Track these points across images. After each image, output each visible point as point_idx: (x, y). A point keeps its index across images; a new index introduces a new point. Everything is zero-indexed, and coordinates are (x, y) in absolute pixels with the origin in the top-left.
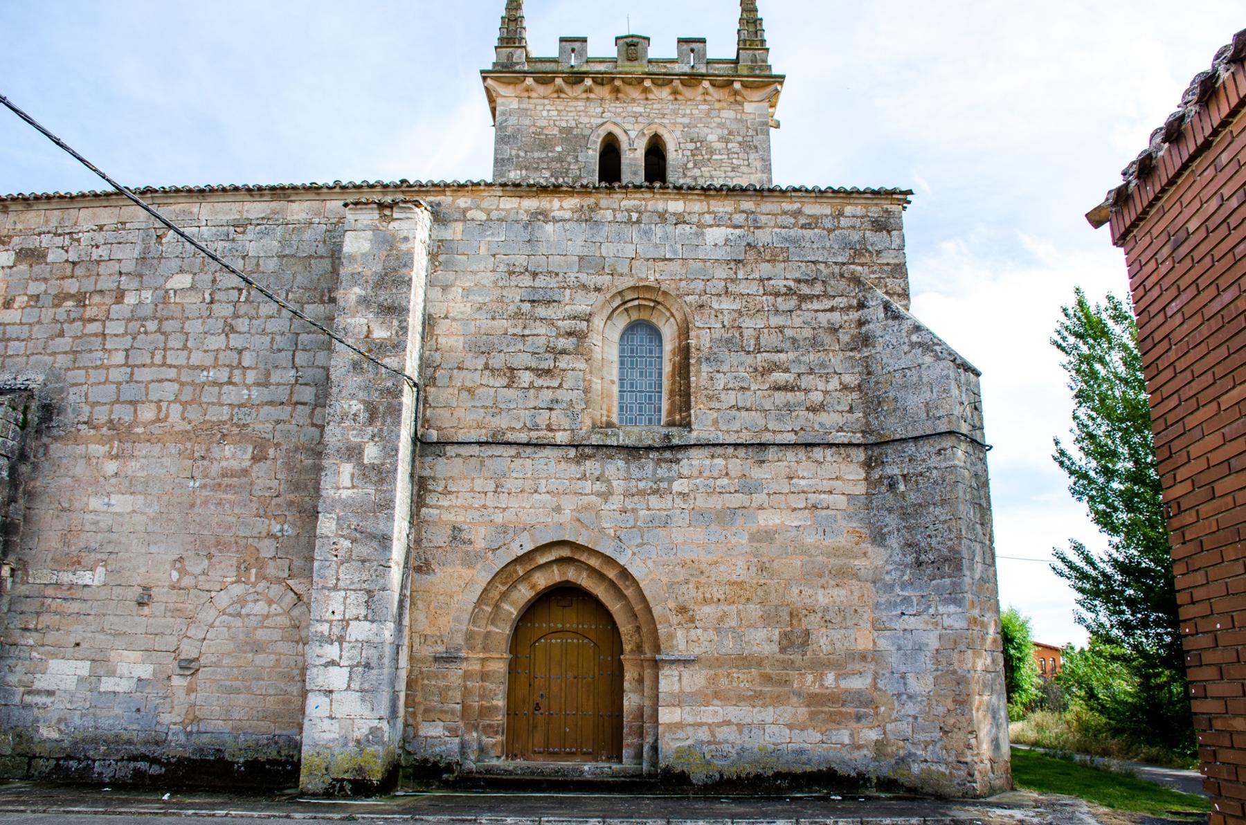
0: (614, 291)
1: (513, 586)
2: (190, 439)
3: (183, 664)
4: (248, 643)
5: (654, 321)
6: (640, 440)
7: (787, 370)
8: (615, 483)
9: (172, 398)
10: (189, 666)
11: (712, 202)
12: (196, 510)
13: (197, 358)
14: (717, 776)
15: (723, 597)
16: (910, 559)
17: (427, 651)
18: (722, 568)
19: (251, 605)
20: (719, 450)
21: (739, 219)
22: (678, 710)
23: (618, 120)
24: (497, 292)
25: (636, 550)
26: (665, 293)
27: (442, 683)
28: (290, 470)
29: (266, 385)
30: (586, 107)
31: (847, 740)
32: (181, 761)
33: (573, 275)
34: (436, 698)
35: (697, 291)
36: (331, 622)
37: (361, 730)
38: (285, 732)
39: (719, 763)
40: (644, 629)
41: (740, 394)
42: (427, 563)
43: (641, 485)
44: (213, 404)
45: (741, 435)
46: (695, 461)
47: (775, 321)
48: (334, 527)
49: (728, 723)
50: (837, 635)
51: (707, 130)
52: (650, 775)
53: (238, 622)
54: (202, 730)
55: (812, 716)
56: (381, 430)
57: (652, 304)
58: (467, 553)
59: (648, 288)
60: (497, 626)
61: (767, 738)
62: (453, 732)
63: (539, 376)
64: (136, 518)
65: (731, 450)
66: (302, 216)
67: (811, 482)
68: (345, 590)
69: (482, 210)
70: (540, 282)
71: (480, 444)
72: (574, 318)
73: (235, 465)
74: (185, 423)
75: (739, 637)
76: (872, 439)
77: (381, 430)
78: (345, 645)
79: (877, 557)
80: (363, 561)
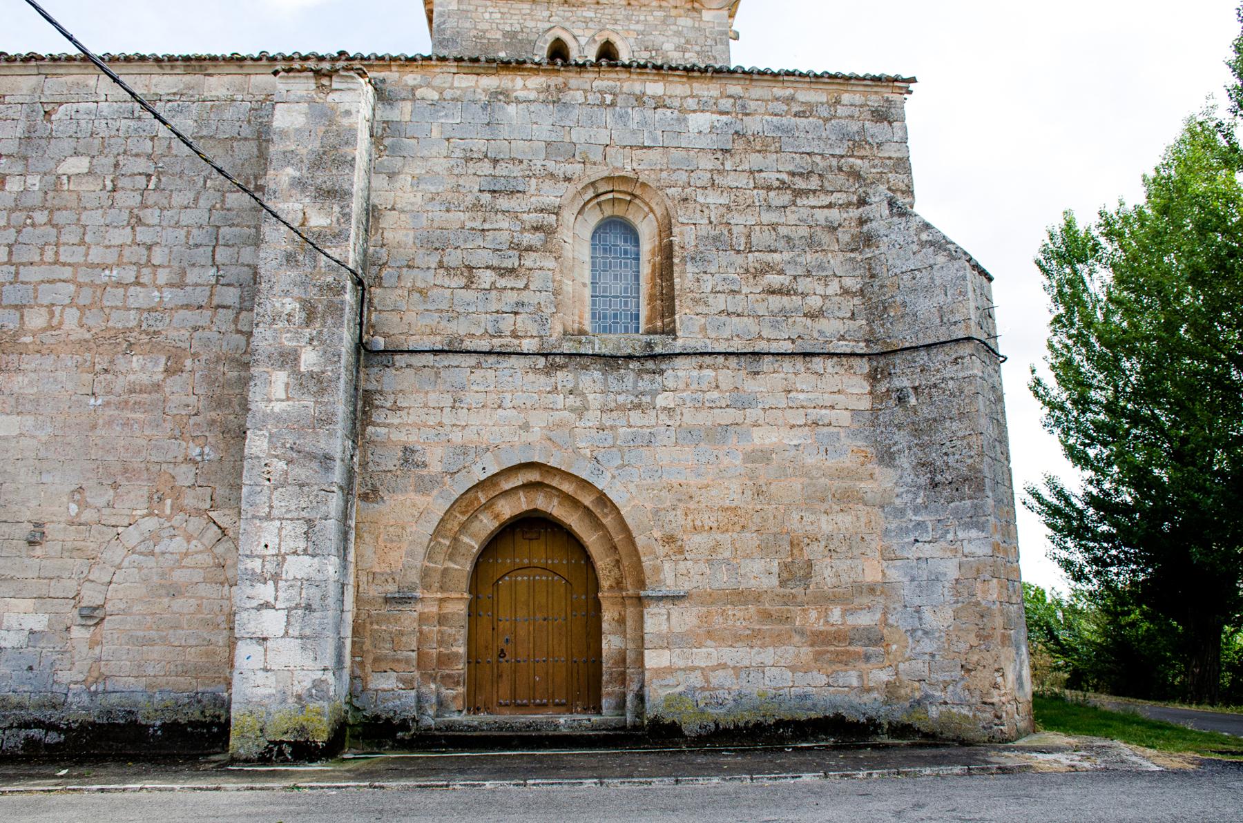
0: (587, 181)
1: (474, 517)
2: (89, 350)
3: (85, 612)
4: (162, 586)
5: (630, 217)
6: (619, 349)
7: (781, 272)
8: (590, 397)
9: (68, 301)
10: (92, 616)
11: (695, 85)
12: (98, 432)
13: (96, 255)
14: (713, 726)
15: (715, 525)
16: (924, 480)
17: (375, 591)
18: (714, 492)
19: (166, 541)
20: (708, 360)
21: (726, 104)
22: (667, 652)
23: (567, 25)
24: (452, 181)
25: (616, 473)
26: (644, 185)
27: (394, 628)
28: (211, 383)
29: (181, 285)
30: (532, 10)
31: (855, 683)
32: (83, 726)
33: (539, 163)
34: (388, 646)
35: (680, 183)
36: (263, 557)
37: (303, 683)
39: (714, 712)
40: (626, 562)
41: (729, 298)
42: (375, 490)
43: (621, 399)
44: (117, 308)
45: (732, 343)
46: (682, 371)
47: (768, 217)
48: (265, 445)
49: (724, 666)
50: (843, 565)
51: (662, 39)
52: (635, 727)
53: (151, 562)
54: (109, 688)
55: (818, 656)
56: (320, 332)
57: (628, 198)
58: (420, 477)
59: (624, 179)
60: (455, 563)
61: (767, 682)
62: (408, 683)
63: (502, 275)
64: (24, 442)
65: (721, 359)
66: (222, 92)
67: (810, 396)
68: (279, 519)
69: (433, 88)
70: (501, 170)
71: (435, 352)
72: (542, 211)
73: (144, 378)
74: (84, 331)
75: (734, 569)
76: (877, 349)
77: (320, 332)
78: (281, 584)
79: (884, 480)
80: (301, 486)
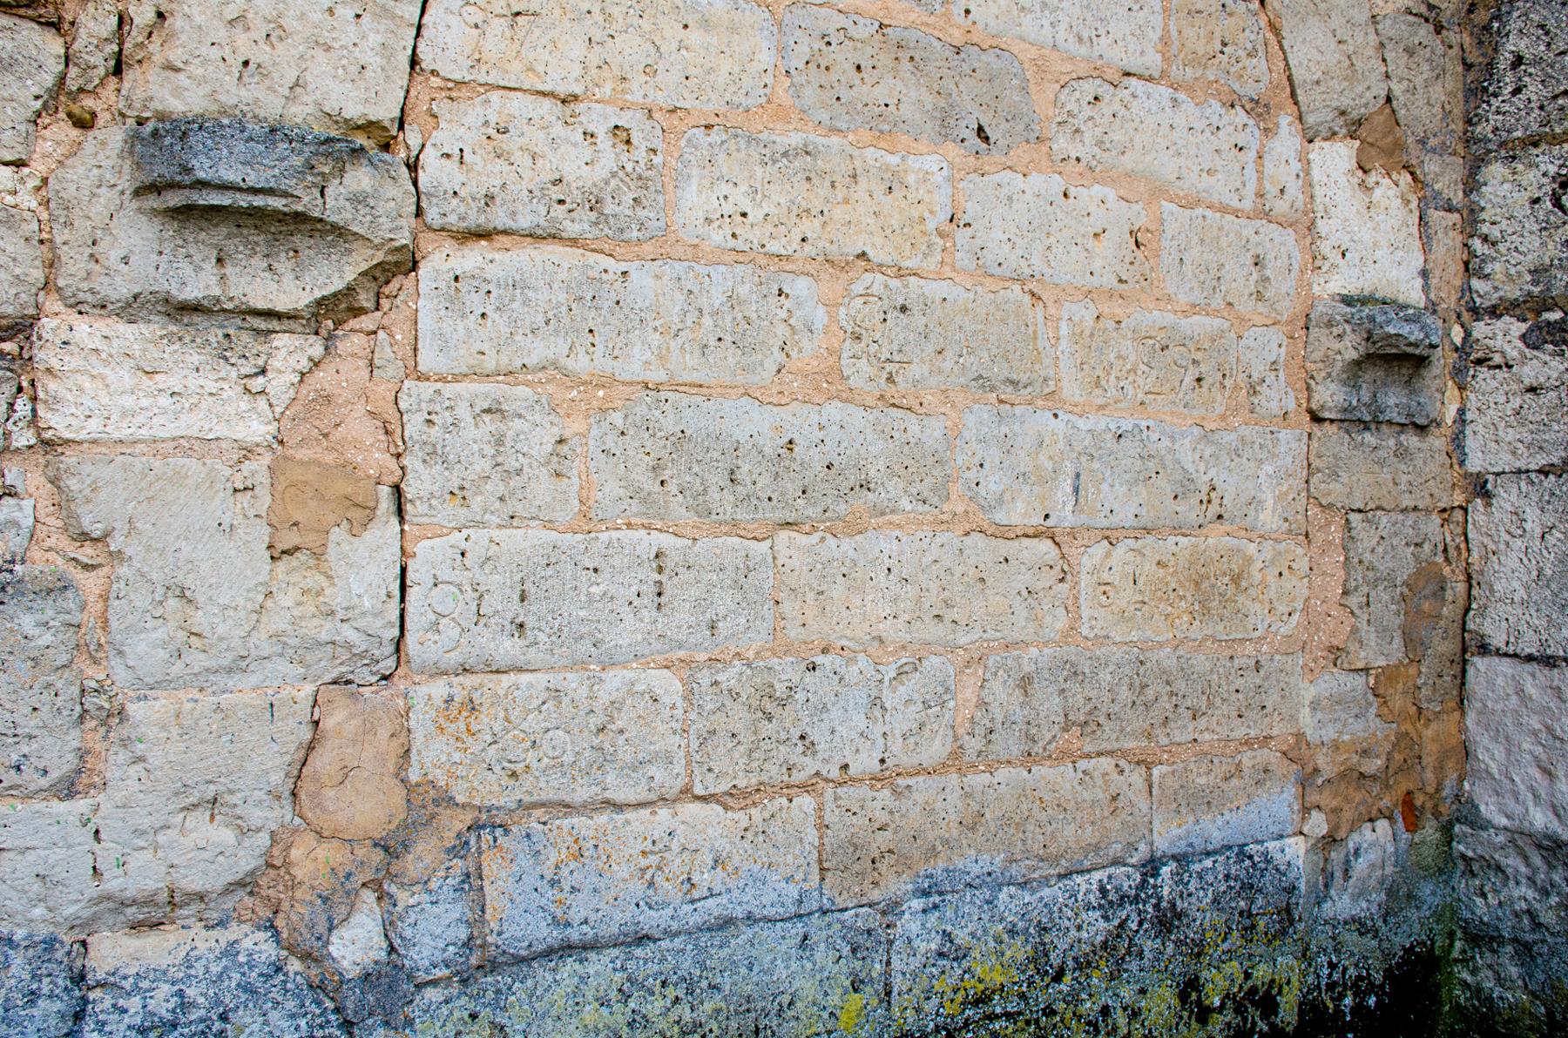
38: (1216, 828)
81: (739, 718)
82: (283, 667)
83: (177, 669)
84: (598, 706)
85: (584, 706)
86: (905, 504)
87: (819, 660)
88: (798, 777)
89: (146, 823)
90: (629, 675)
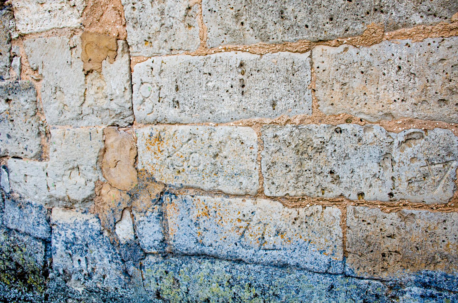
54: (182, 239)
81: (289, 156)
82: (93, 118)
83: (62, 118)
84: (214, 144)
85: (207, 142)
86: (416, 18)
87: (344, 126)
88: (328, 195)
89: (59, 172)
90: (228, 129)
